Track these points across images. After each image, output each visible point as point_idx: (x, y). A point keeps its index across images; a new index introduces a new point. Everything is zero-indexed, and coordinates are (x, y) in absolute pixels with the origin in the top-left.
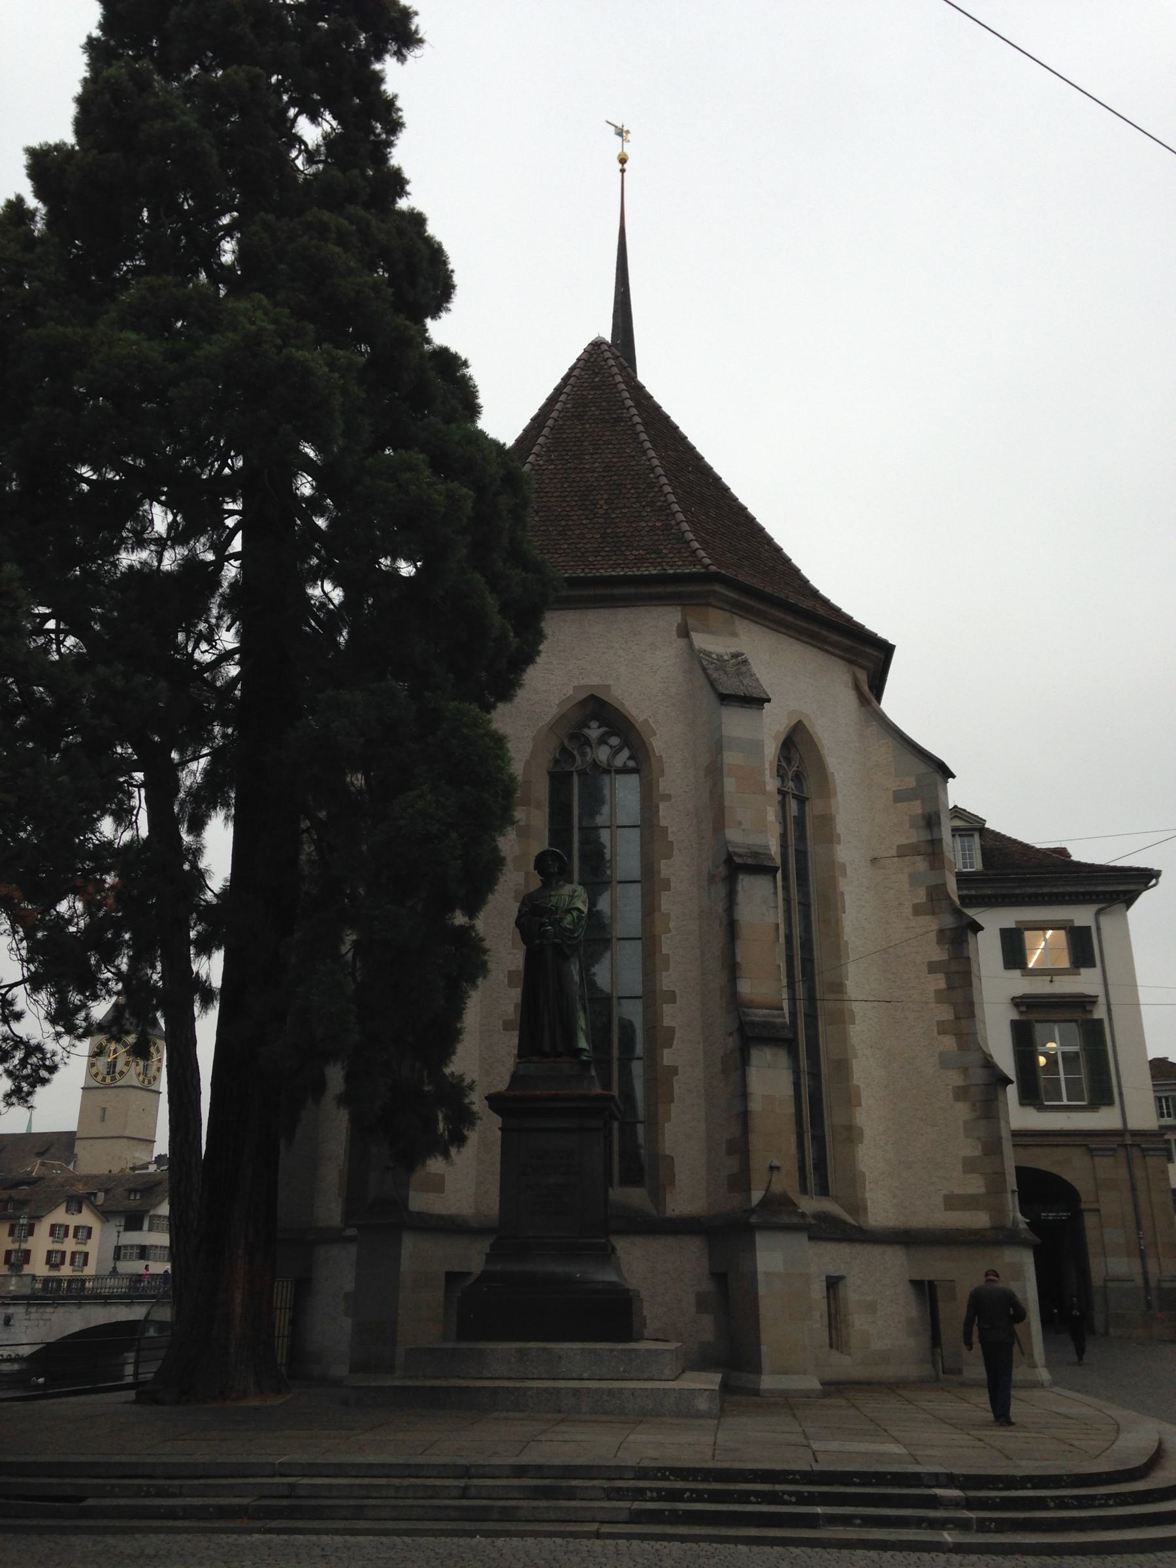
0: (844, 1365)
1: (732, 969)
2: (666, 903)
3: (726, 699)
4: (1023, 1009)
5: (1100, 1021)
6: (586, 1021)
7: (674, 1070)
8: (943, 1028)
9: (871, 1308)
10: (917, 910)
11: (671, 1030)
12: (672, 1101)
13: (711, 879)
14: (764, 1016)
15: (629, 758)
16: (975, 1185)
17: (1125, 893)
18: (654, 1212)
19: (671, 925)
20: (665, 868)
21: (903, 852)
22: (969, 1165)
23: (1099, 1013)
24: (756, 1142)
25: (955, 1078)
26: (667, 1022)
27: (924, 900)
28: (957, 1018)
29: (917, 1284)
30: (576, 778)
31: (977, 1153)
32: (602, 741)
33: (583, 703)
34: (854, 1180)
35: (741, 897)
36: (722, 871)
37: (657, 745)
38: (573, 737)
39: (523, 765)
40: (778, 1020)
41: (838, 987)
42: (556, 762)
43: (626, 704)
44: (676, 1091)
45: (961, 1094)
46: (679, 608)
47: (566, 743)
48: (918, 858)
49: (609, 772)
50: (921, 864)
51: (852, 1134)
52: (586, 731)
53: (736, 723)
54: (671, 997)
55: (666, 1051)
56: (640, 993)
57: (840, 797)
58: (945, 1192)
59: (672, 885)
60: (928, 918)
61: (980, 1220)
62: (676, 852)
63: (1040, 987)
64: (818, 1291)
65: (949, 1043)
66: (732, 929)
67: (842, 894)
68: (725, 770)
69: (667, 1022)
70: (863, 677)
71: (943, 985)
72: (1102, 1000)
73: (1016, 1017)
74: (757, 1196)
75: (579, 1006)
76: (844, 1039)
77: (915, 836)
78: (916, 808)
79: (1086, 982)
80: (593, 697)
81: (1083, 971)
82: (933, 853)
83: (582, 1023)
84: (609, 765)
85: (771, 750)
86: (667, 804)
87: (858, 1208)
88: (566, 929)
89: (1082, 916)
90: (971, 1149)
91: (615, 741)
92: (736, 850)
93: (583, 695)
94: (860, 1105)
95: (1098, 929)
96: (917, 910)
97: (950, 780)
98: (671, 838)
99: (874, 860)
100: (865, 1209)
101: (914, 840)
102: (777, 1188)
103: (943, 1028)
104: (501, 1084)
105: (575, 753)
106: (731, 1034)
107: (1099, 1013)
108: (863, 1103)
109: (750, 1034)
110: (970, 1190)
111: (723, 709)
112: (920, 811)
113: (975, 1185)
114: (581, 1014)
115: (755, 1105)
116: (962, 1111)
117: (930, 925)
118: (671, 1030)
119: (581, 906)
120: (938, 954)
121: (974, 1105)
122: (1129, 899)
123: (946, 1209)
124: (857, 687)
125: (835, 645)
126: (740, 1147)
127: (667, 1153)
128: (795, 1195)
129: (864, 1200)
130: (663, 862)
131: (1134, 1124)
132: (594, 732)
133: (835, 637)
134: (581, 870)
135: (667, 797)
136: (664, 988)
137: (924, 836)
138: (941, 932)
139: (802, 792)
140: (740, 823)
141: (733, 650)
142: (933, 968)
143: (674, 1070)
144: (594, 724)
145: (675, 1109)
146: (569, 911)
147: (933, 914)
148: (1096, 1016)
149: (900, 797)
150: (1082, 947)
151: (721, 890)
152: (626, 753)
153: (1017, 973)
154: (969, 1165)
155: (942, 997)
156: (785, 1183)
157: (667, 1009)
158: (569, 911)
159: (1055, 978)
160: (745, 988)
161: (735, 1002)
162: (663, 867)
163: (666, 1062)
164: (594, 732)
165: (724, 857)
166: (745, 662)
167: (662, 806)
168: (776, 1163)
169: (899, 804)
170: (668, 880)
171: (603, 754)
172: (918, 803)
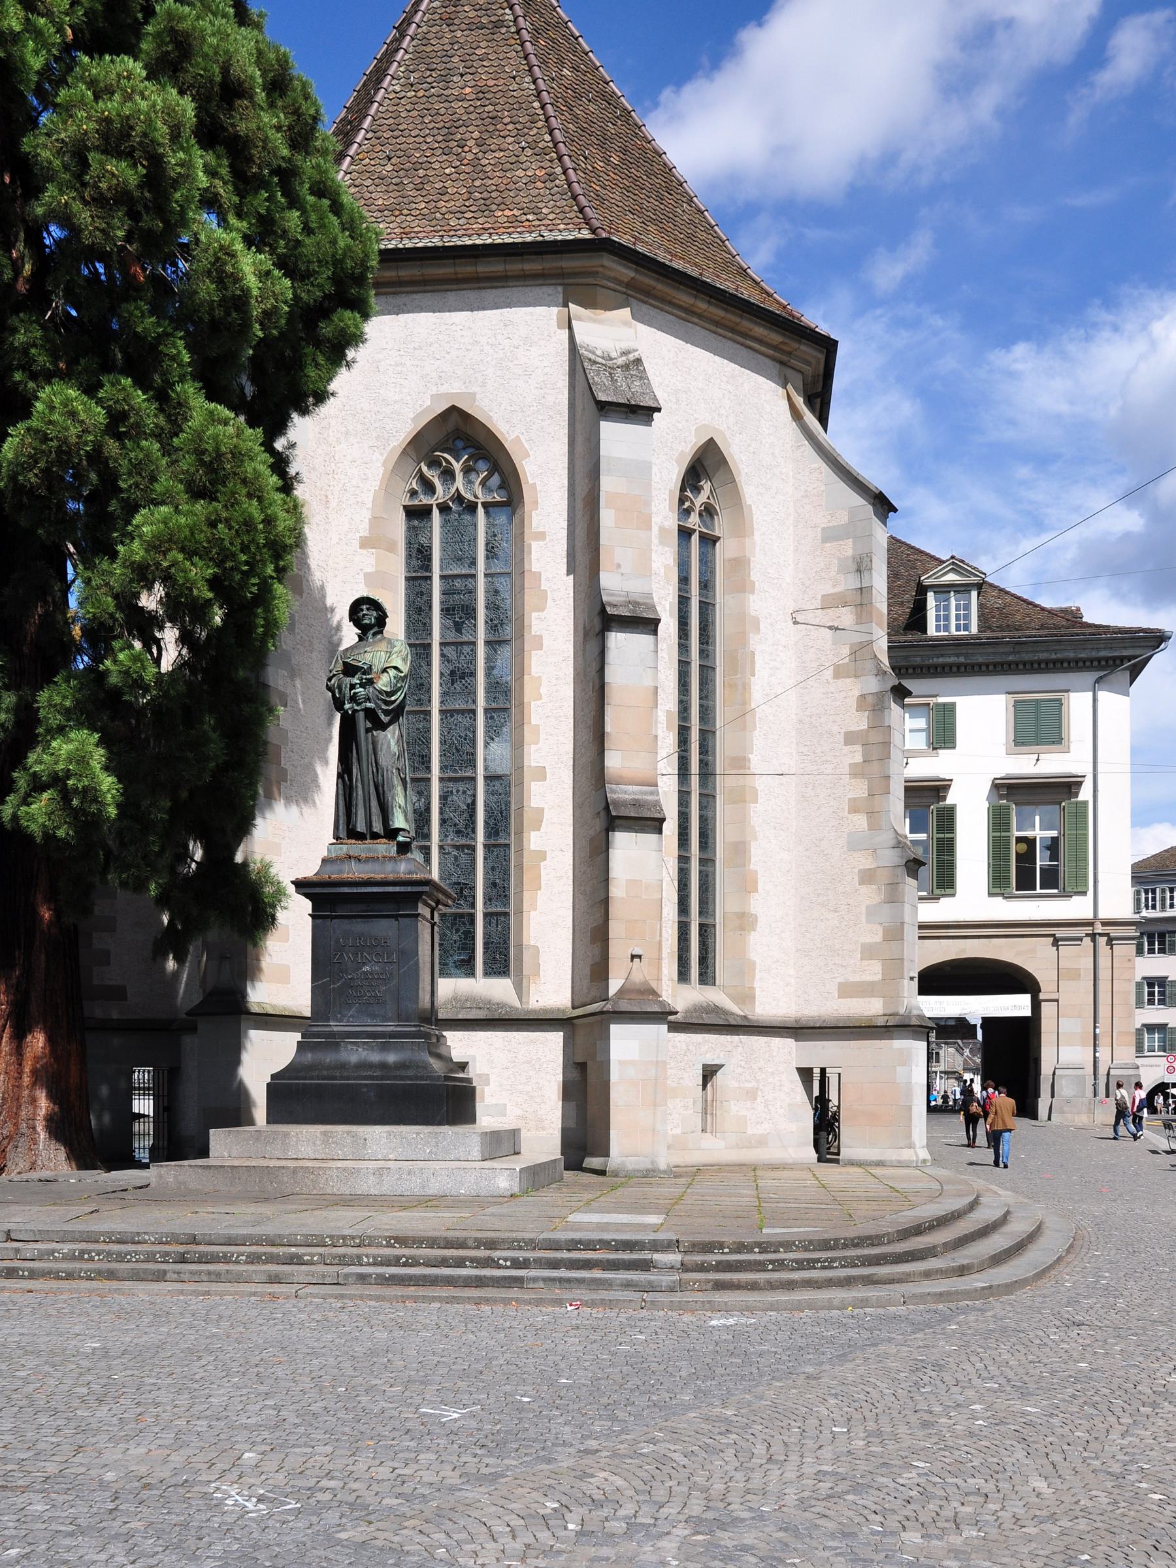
7: (542, 855)
10: (839, 672)
11: (541, 811)
19: (543, 690)
21: (830, 602)
30: (436, 512)
31: (878, 938)
34: (746, 969)
35: (612, 656)
40: (650, 798)
41: (740, 763)
43: (495, 417)
46: (560, 289)
51: (745, 922)
55: (533, 834)
57: (757, 536)
65: (860, 821)
67: (753, 653)
75: (396, 781)
76: (742, 821)
80: (453, 408)
83: (400, 799)
86: (541, 543)
87: (747, 997)
96: (839, 672)
97: (891, 514)
113: (873, 971)
114: (399, 789)
115: (617, 891)
116: (870, 895)
118: (541, 811)
120: (860, 722)
129: (752, 989)
130: (534, 615)
134: (444, 627)
135: (541, 536)
136: (533, 764)
137: (852, 582)
138: (863, 696)
140: (619, 566)
143: (542, 855)
146: (385, 670)
149: (830, 535)
151: (593, 646)
158: (385, 670)
163: (533, 847)
165: (598, 608)
168: (637, 952)
169: (828, 545)
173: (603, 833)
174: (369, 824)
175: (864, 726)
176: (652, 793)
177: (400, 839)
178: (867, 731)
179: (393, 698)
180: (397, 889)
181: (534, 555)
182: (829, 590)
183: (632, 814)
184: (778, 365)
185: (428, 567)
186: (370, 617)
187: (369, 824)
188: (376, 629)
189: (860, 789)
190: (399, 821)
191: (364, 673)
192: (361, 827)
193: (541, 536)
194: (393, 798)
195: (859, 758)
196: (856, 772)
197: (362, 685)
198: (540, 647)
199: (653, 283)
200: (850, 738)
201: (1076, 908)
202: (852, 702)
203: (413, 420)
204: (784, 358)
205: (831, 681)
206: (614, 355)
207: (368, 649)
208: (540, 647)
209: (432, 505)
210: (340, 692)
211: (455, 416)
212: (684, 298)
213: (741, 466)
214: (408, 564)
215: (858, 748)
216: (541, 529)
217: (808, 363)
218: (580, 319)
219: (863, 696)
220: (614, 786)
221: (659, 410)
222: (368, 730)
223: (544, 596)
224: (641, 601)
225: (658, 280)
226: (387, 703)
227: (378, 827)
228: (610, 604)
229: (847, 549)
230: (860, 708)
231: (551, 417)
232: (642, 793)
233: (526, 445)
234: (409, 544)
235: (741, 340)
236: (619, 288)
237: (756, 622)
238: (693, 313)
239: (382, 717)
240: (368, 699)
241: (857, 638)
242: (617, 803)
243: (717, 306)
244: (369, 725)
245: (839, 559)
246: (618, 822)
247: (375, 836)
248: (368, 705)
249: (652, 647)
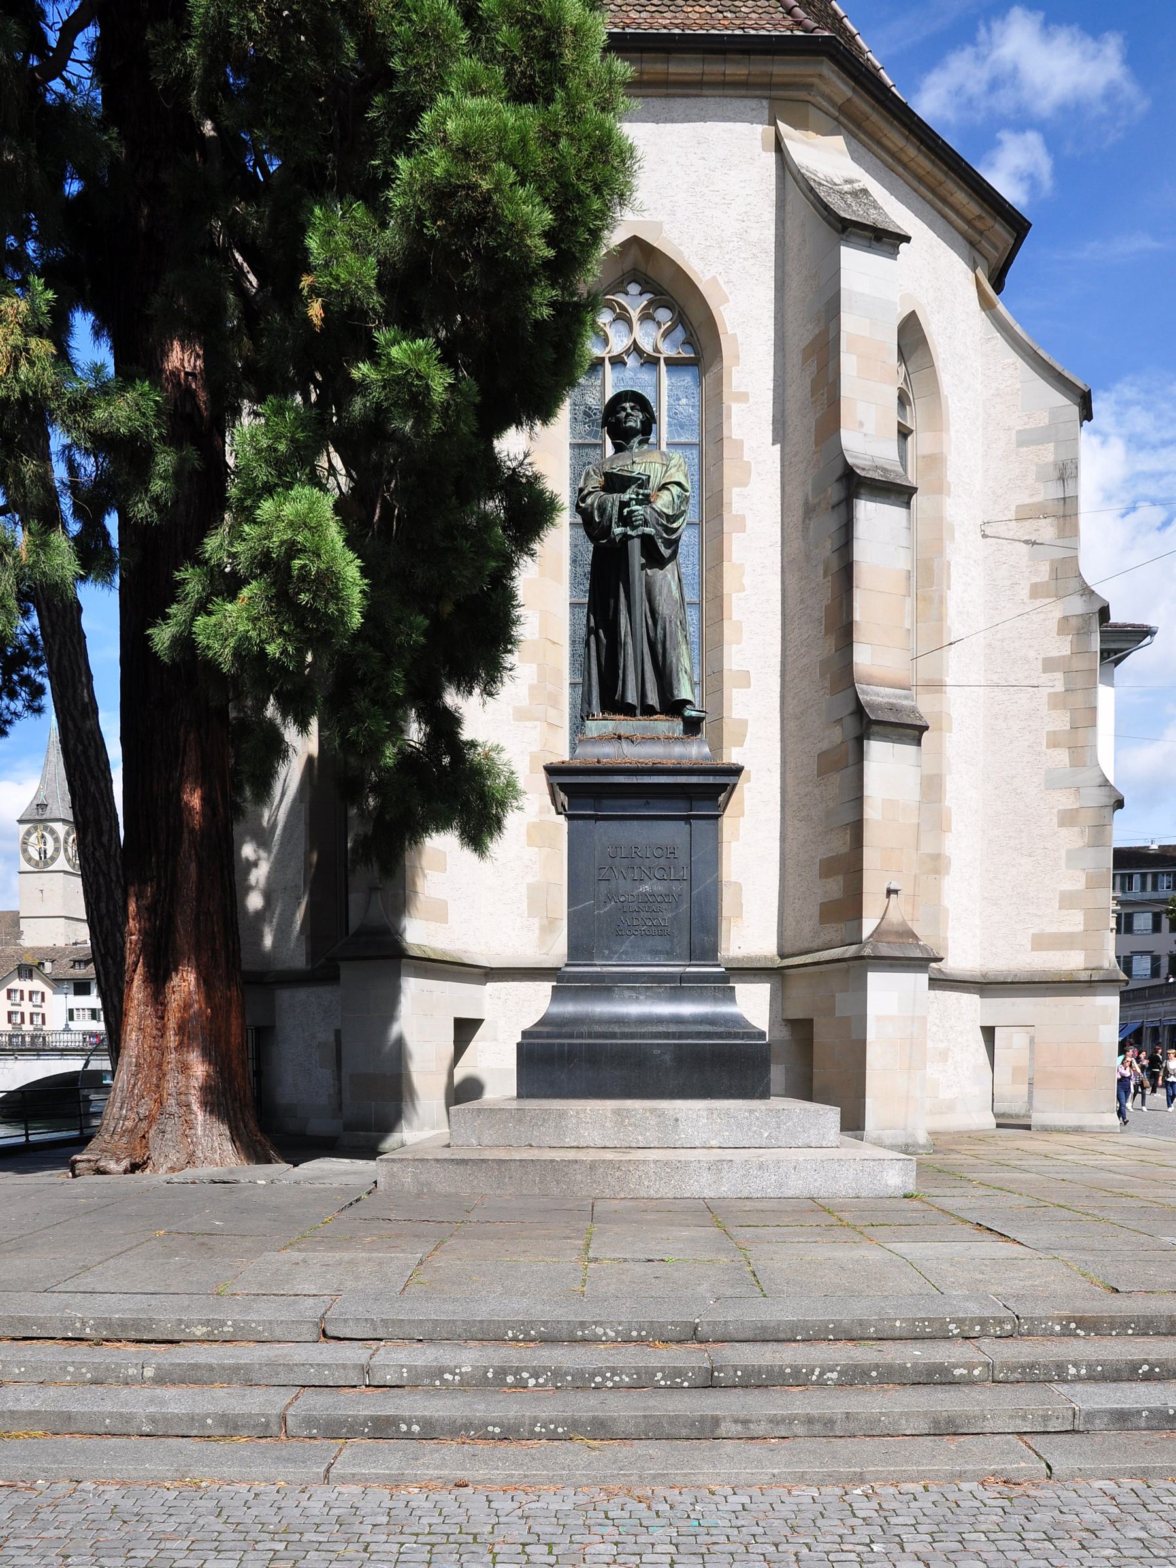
10: (1036, 591)
11: (744, 723)
12: (743, 815)
13: (809, 511)
14: (887, 696)
19: (745, 581)
21: (1025, 514)
27: (1046, 578)
36: (835, 493)
40: (905, 703)
48: (1043, 522)
52: (620, 298)
59: (749, 524)
96: (1036, 591)
101: (1039, 498)
112: (1051, 458)
118: (744, 723)
127: (733, 879)
130: (736, 490)
133: (960, 197)
135: (743, 397)
136: (735, 668)
137: (1054, 491)
140: (861, 424)
144: (634, 289)
146: (664, 487)
158: (664, 487)
162: (735, 499)
165: (839, 472)
170: (743, 517)
173: (851, 745)
174: (643, 695)
175: (1066, 651)
176: (906, 698)
178: (1070, 658)
179: (675, 525)
180: (694, 780)
181: (734, 419)
183: (892, 720)
184: (968, 246)
186: (635, 421)
187: (643, 695)
188: (640, 437)
189: (1061, 721)
191: (640, 486)
192: (632, 698)
194: (678, 659)
195: (1060, 687)
196: (1056, 702)
197: (639, 502)
199: (868, 110)
200: (1049, 665)
202: (1053, 625)
204: (977, 238)
205: (1027, 601)
206: (838, 182)
207: (637, 459)
209: (603, 359)
210: (601, 515)
211: (634, 251)
212: (895, 138)
213: (939, 350)
214: (573, 429)
215: (1059, 676)
216: (742, 390)
217: (996, 248)
219: (1066, 618)
220: (864, 686)
221: (907, 239)
222: (643, 567)
223: (747, 469)
224: (889, 467)
225: (873, 108)
227: (653, 699)
229: (1048, 454)
230: (1061, 631)
231: (755, 256)
232: (896, 697)
233: (724, 287)
235: (940, 205)
236: (831, 109)
238: (899, 161)
239: (662, 549)
240: (646, 523)
241: (1060, 554)
242: (872, 706)
243: (926, 156)
244: (644, 561)
245: (1037, 464)
246: (875, 728)
247: (648, 711)
248: (647, 530)
249: (904, 523)
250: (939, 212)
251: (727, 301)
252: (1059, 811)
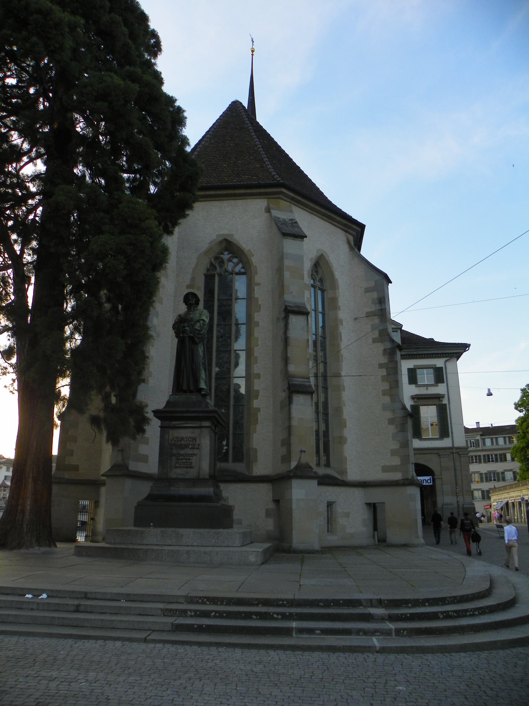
0: (333, 540)
1: (286, 360)
2: (257, 333)
3: (285, 235)
4: (416, 400)
5: (446, 404)
6: (206, 375)
7: (258, 410)
8: (384, 393)
9: (347, 515)
11: (258, 391)
15: (242, 268)
16: (396, 461)
17: (456, 353)
18: (247, 474)
19: (259, 343)
20: (257, 317)
22: (393, 453)
23: (445, 401)
24: (294, 440)
25: (389, 415)
26: (256, 388)
28: (391, 388)
29: (368, 504)
32: (230, 260)
33: (221, 242)
34: (343, 460)
35: (290, 326)
36: (283, 315)
37: (254, 260)
38: (216, 258)
39: (191, 270)
40: (307, 384)
42: (208, 270)
44: (259, 419)
45: (391, 421)
47: (213, 261)
49: (232, 274)
50: (376, 320)
51: (342, 440)
52: (222, 256)
53: (290, 246)
54: (258, 376)
55: (255, 401)
56: (244, 376)
57: (340, 290)
58: (383, 465)
59: (260, 324)
60: (379, 344)
61: (398, 476)
62: (262, 309)
63: (423, 391)
64: (323, 508)
65: (387, 399)
66: (286, 341)
67: (341, 333)
68: (285, 268)
69: (256, 388)
70: (351, 238)
71: (385, 373)
72: (446, 396)
73: (413, 404)
74: (294, 464)
77: (374, 308)
78: (375, 295)
79: (441, 389)
81: (439, 384)
82: (382, 315)
84: (232, 271)
85: (308, 265)
87: (344, 472)
88: (196, 330)
89: (439, 362)
90: (395, 446)
91: (235, 260)
92: (288, 304)
93: (221, 238)
94: (346, 427)
95: (446, 368)
97: (390, 284)
98: (260, 302)
99: (356, 319)
100: (347, 472)
102: (303, 461)
103: (384, 393)
104: (161, 406)
105: (217, 266)
106: (284, 391)
107: (445, 401)
108: (347, 426)
109: (294, 388)
110: (393, 464)
111: (284, 240)
113: (396, 461)
115: (294, 423)
116: (392, 429)
117: (380, 347)
118: (258, 391)
119: (204, 318)
120: (384, 360)
121: (397, 426)
122: (458, 356)
123: (382, 472)
124: (348, 242)
125: (339, 222)
126: (287, 443)
127: (254, 447)
128: (313, 464)
129: (346, 469)
130: (256, 314)
131: (456, 445)
132: (226, 256)
135: (259, 284)
136: (255, 372)
138: (385, 350)
139: (323, 286)
140: (291, 293)
141: (290, 218)
142: (381, 366)
143: (258, 410)
144: (226, 253)
145: (259, 427)
146: (198, 321)
147: (382, 342)
148: (444, 403)
150: (440, 376)
151: (282, 324)
152: (240, 265)
153: (413, 386)
154: (393, 453)
155: (384, 379)
156: (310, 459)
157: (256, 381)
158: (198, 321)
159: (429, 388)
160: (292, 368)
161: (287, 375)
162: (256, 316)
163: (255, 406)
164: (226, 256)
165: (283, 308)
166: (296, 222)
167: (256, 288)
168: (303, 449)
169: (367, 294)
170: (258, 322)
171: (230, 266)
172: (376, 293)
173: (287, 399)
177: (203, 393)
182: (368, 310)
185: (213, 297)
190: (203, 385)
192: (185, 387)
193: (259, 284)
198: (258, 326)
201: (446, 443)
203: (209, 243)
208: (258, 326)
218: (273, 209)
221: (306, 237)
223: (260, 306)
226: (198, 334)
228: (289, 306)
234: (205, 288)
237: (341, 322)
247: (191, 392)
250: (332, 224)
251: (253, 255)
252: (388, 419)
